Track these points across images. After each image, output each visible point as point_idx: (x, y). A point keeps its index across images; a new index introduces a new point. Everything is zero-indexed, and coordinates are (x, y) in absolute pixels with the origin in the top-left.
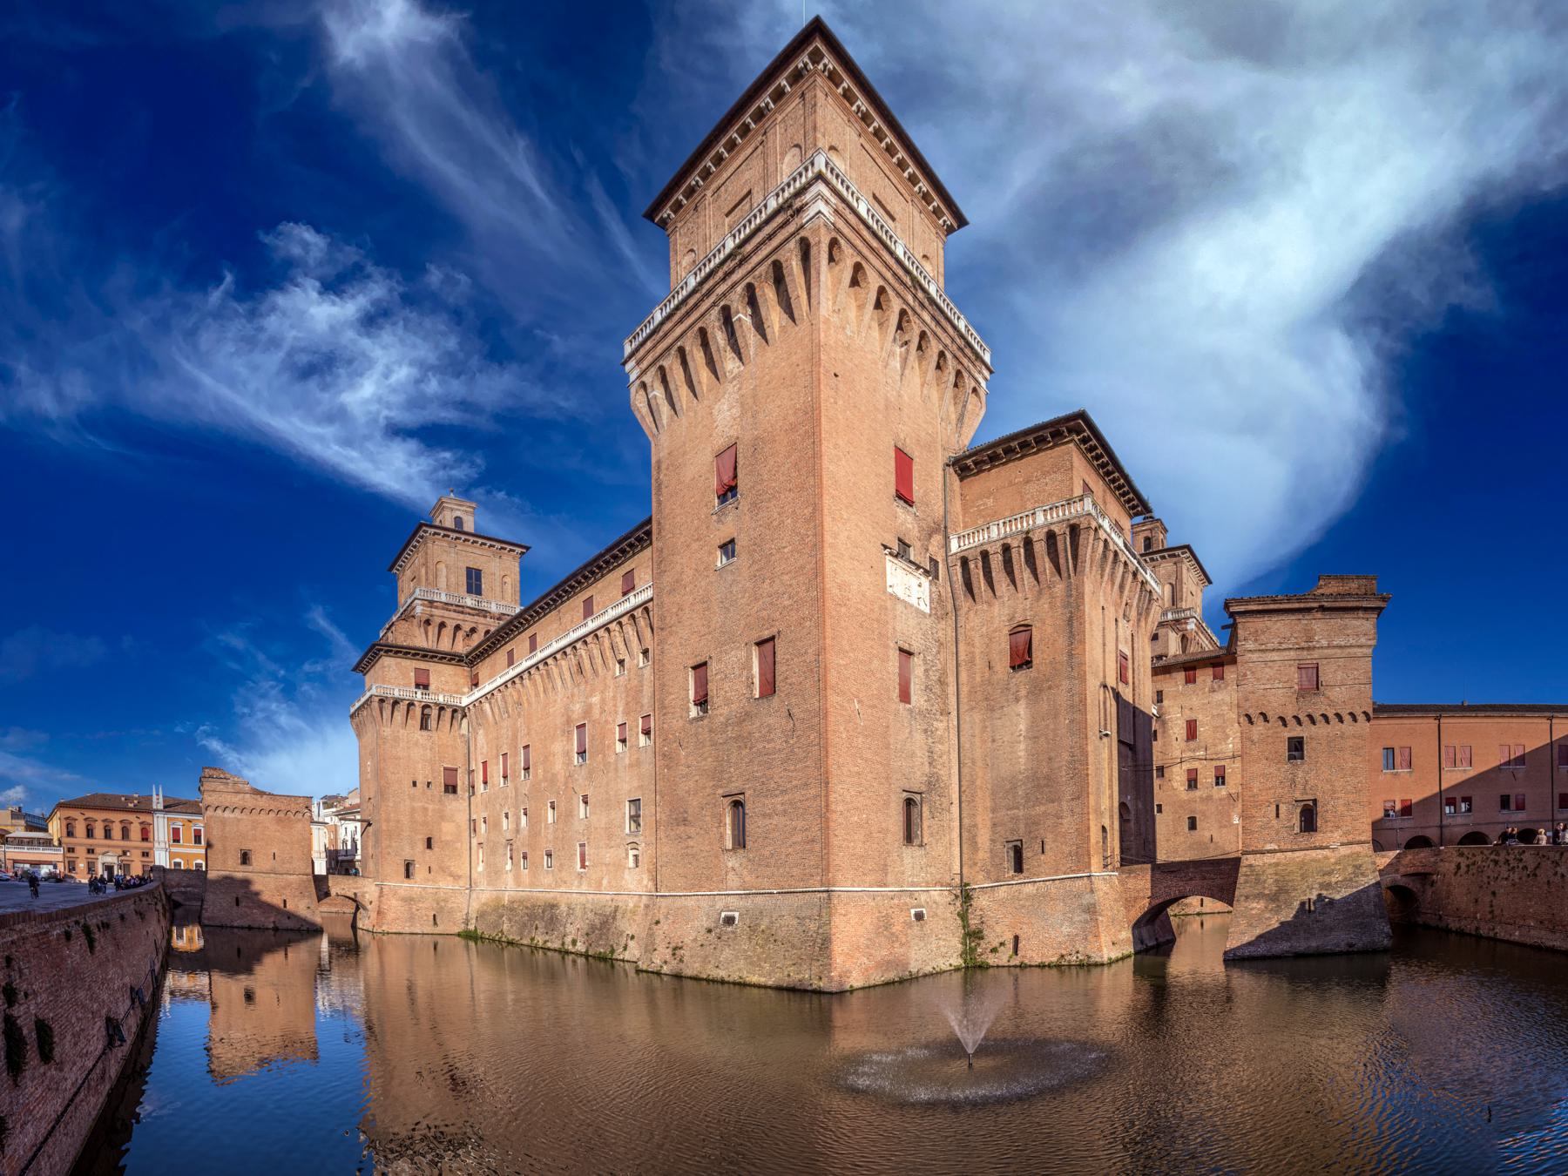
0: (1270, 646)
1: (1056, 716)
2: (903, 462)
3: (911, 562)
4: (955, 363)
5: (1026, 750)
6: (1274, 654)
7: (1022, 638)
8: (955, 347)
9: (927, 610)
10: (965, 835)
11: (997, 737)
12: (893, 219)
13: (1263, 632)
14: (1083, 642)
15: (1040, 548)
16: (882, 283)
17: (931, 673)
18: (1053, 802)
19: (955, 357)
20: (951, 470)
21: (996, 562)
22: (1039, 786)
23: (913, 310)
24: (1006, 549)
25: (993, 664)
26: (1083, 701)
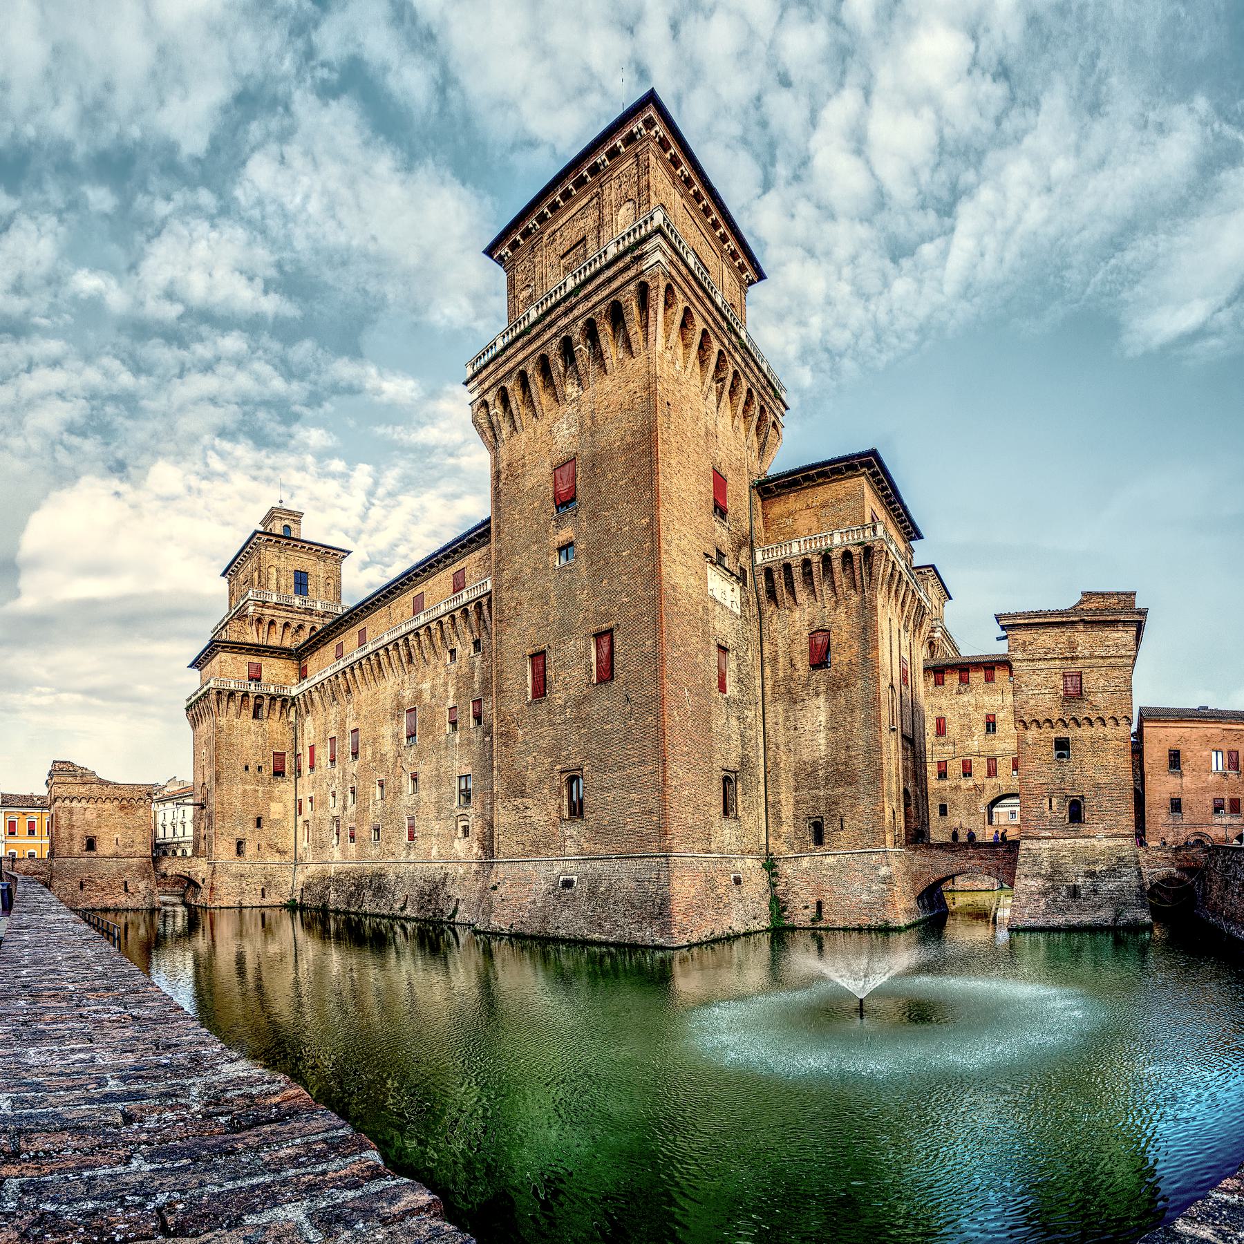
0: (1037, 656)
1: (852, 711)
2: (720, 482)
3: (726, 569)
6: (1040, 663)
9: (738, 612)
10: (770, 810)
11: (799, 725)
13: (1031, 644)
14: (876, 648)
16: (705, 327)
19: (759, 393)
21: (797, 573)
24: (807, 563)
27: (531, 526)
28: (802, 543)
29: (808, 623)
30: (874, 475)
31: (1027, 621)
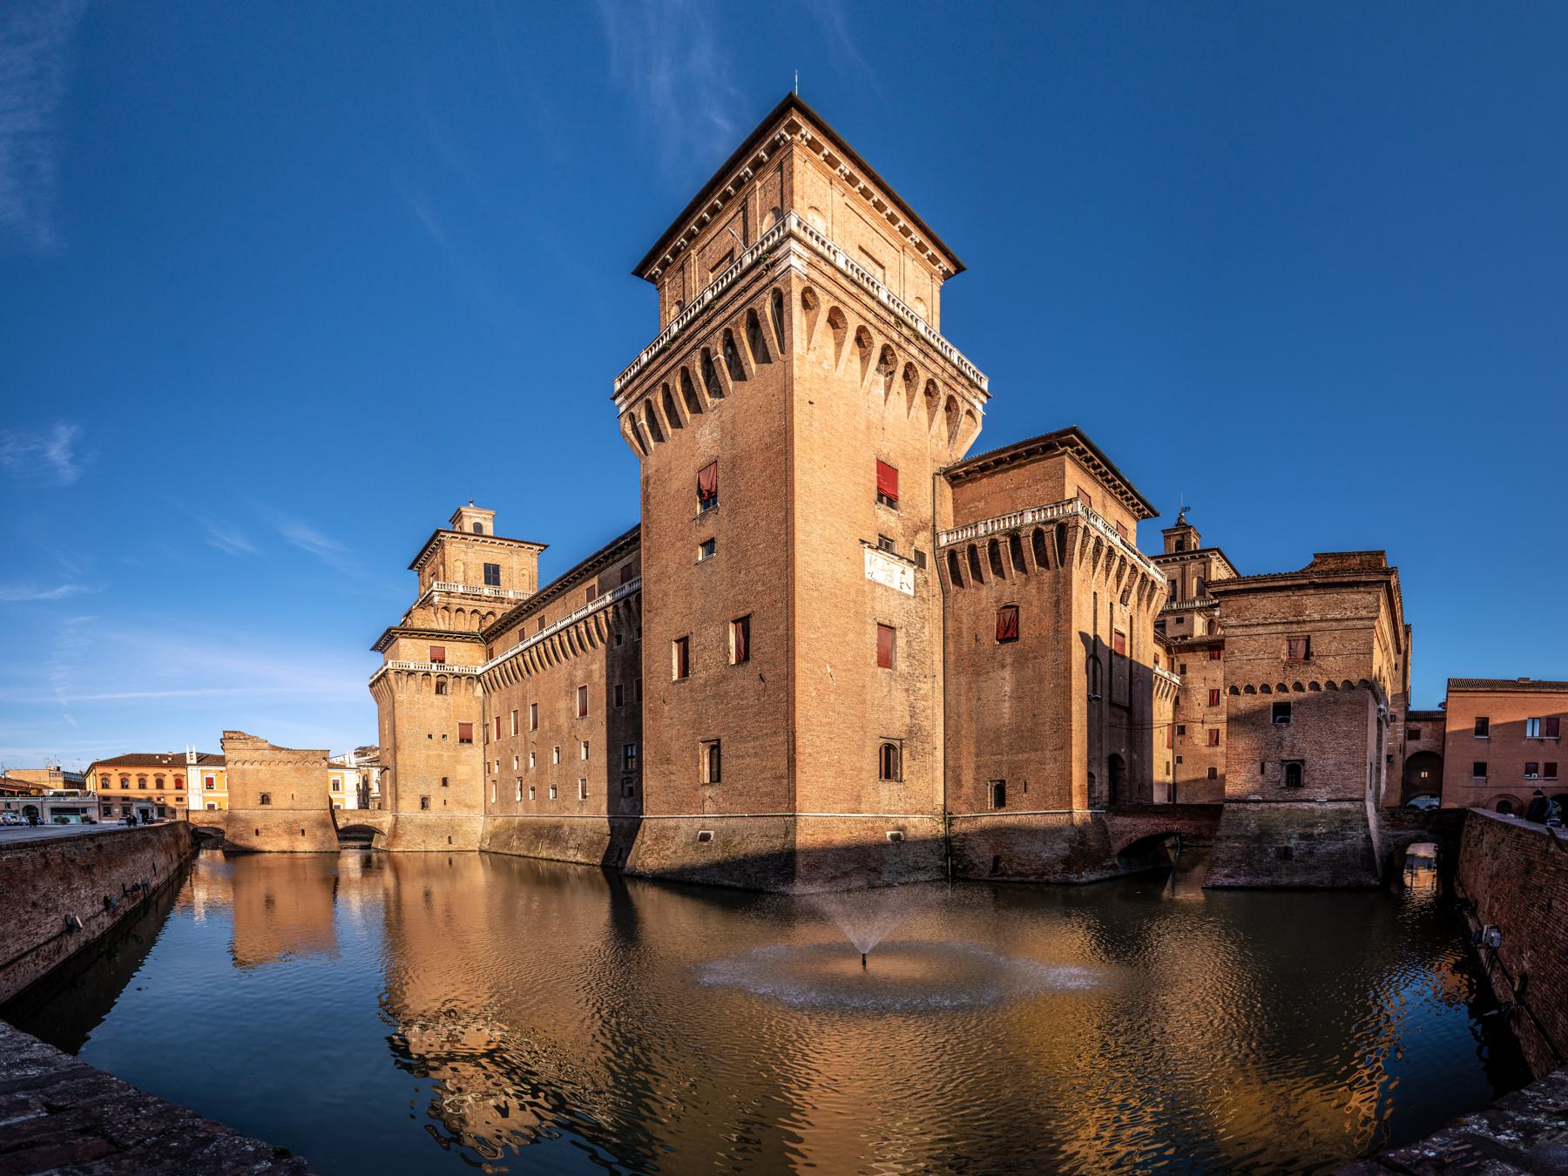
4: (946, 388)
5: (1011, 707)
7: (1009, 614)
8: (946, 375)
9: (911, 593)
11: (983, 696)
12: (882, 267)
18: (1036, 750)
19: (946, 384)
20: (942, 479)
21: (983, 554)
22: (1022, 737)
24: (994, 544)
25: (979, 637)
26: (1068, 669)
28: (989, 524)
31: (1242, 587)
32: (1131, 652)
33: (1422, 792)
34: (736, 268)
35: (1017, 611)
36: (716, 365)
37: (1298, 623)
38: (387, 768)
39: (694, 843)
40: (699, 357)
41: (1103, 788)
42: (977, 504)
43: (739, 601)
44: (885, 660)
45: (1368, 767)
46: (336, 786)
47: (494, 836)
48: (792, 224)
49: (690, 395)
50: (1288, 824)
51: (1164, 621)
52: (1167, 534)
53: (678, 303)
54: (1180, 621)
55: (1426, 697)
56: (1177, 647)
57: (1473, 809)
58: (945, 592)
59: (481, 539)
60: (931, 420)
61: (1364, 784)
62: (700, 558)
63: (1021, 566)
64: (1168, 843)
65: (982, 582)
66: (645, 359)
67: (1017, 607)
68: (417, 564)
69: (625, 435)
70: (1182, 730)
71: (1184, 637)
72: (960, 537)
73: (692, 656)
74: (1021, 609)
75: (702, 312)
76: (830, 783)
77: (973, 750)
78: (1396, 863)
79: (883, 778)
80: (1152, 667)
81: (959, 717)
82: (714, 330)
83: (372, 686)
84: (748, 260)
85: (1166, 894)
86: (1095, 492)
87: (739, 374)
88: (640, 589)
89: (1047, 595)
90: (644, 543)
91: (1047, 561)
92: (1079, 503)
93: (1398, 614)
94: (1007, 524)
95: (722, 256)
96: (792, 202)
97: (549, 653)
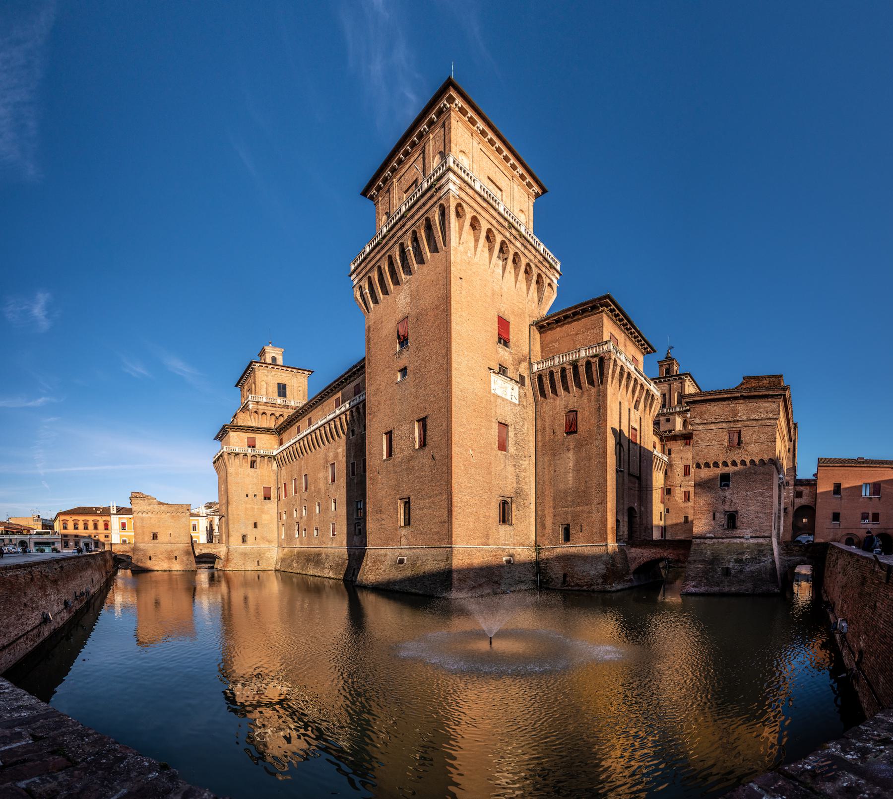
1: (590, 460)
9: (517, 402)
11: (557, 469)
15: (582, 370)
17: (519, 435)
19: (536, 266)
20: (535, 328)
21: (557, 377)
22: (579, 496)
23: (510, 241)
24: (563, 370)
26: (605, 452)
27: (385, 358)
28: (561, 357)
29: (564, 406)
30: (612, 311)
32: (640, 441)
33: (803, 532)
34: (419, 191)
35: (576, 414)
36: (407, 254)
37: (734, 421)
38: (223, 516)
39: (395, 564)
40: (398, 249)
41: (625, 529)
42: (554, 344)
43: (421, 408)
44: (503, 447)
45: (773, 515)
46: (194, 528)
47: (283, 560)
48: (450, 161)
49: (393, 273)
50: (728, 552)
51: (659, 420)
52: (660, 363)
53: (386, 213)
54: (668, 420)
55: (806, 472)
56: (667, 438)
57: (832, 543)
58: (536, 402)
59: (276, 367)
60: (528, 289)
61: (771, 526)
62: (399, 380)
63: (579, 385)
64: (661, 565)
65: (557, 396)
66: (368, 250)
67: (577, 411)
68: (239, 383)
69: (357, 300)
70: (669, 492)
71: (670, 431)
72: (544, 366)
73: (394, 443)
74: (578, 413)
75: (400, 219)
76: (472, 526)
77: (551, 504)
78: (789, 578)
79: (501, 522)
80: (652, 451)
81: (544, 483)
82: (407, 231)
83: (214, 463)
84: (425, 186)
85: (660, 598)
86: (621, 336)
87: (421, 261)
88: (365, 400)
89: (593, 403)
90: (368, 370)
91: (593, 381)
92: (611, 344)
93: (790, 416)
94: (571, 357)
95: (411, 183)
96: (450, 148)
97: (314, 442)
